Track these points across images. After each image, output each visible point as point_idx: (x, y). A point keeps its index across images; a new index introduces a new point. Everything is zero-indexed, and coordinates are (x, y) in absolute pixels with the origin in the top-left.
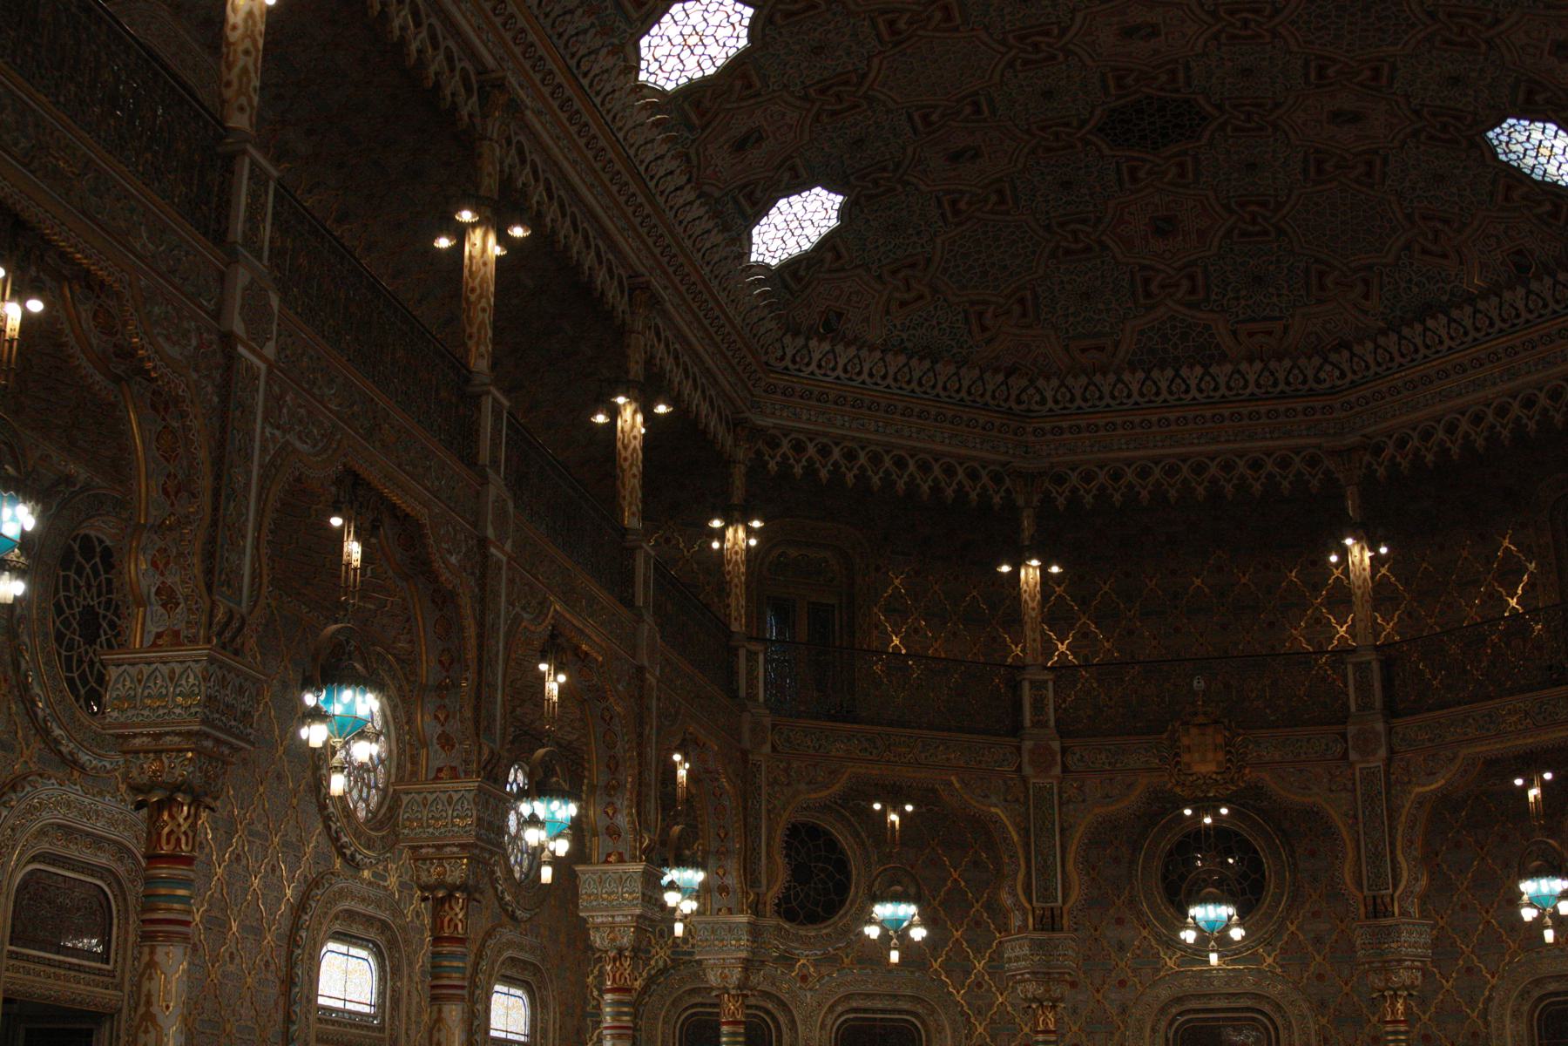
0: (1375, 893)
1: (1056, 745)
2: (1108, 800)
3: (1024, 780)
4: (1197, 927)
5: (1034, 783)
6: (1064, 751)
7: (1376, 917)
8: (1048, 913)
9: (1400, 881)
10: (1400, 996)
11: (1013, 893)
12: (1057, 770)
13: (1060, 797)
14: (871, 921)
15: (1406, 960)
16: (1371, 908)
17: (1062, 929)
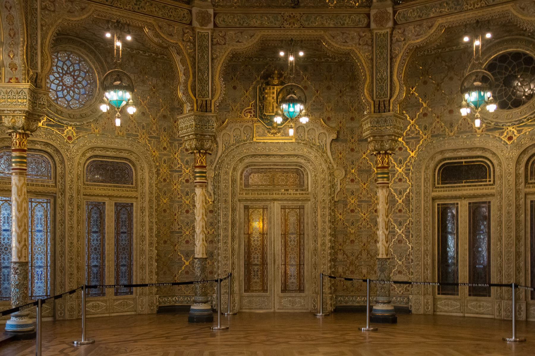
0: (378, 99)
1: (211, 11)
2: (238, 44)
3: (193, 29)
4: (283, 116)
5: (198, 32)
6: (215, 15)
7: (379, 112)
8: (204, 103)
9: (394, 93)
10: (388, 154)
11: (185, 93)
12: (211, 26)
13: (212, 41)
14: (103, 102)
15: (393, 135)
16: (377, 108)
17: (211, 112)
